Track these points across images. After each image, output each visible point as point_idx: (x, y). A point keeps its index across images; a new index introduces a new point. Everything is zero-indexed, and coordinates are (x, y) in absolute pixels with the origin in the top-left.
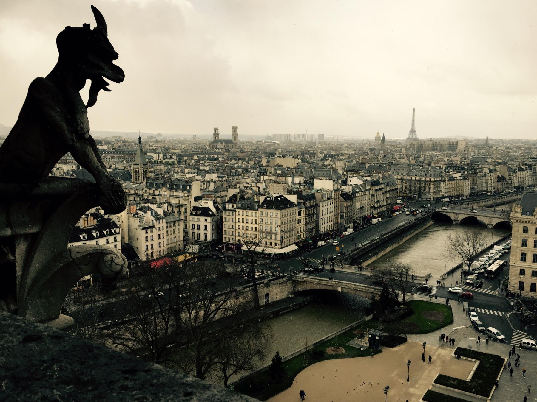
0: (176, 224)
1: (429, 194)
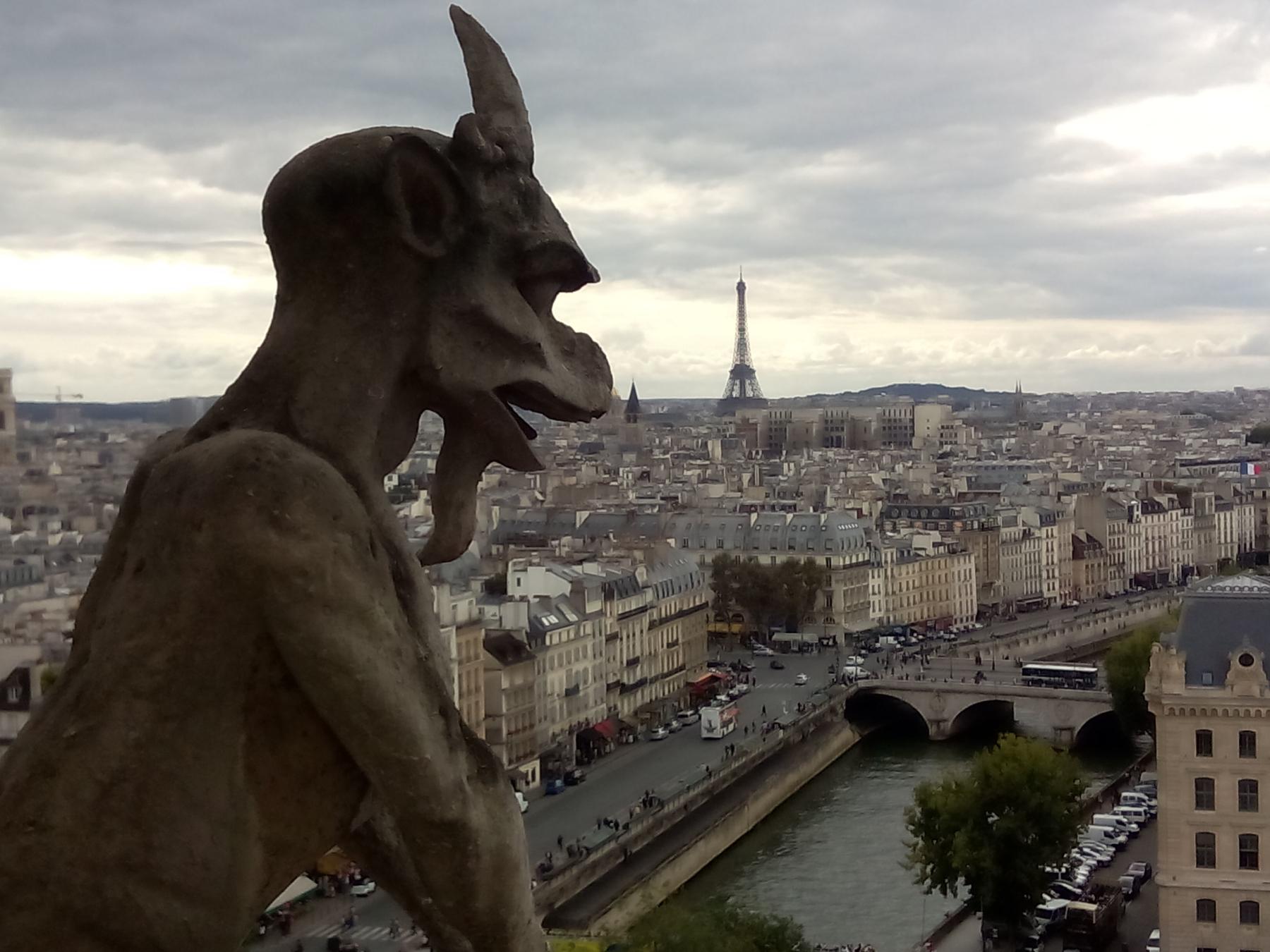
1: (830, 620)
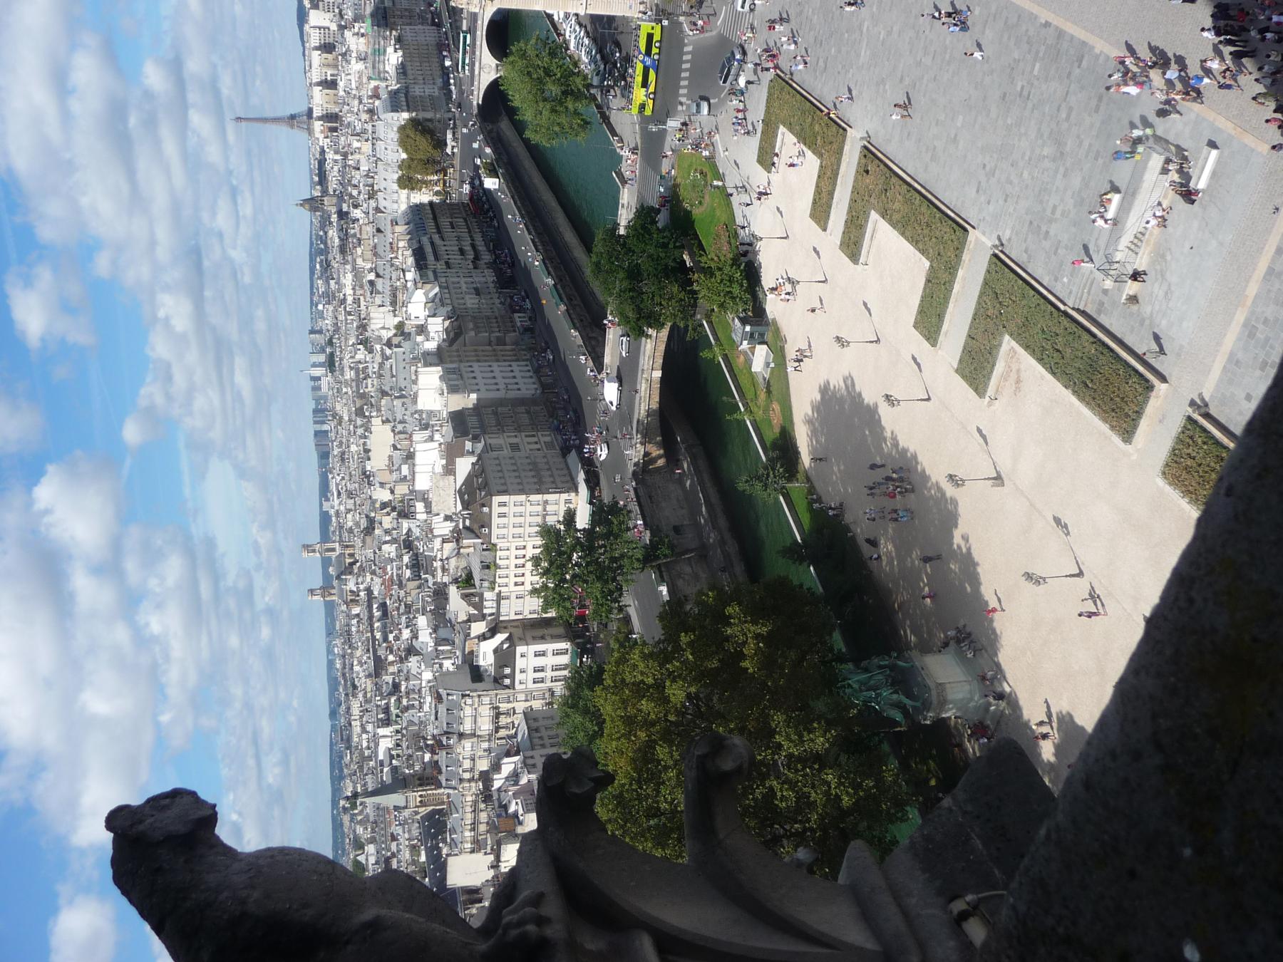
0: (534, 725)
